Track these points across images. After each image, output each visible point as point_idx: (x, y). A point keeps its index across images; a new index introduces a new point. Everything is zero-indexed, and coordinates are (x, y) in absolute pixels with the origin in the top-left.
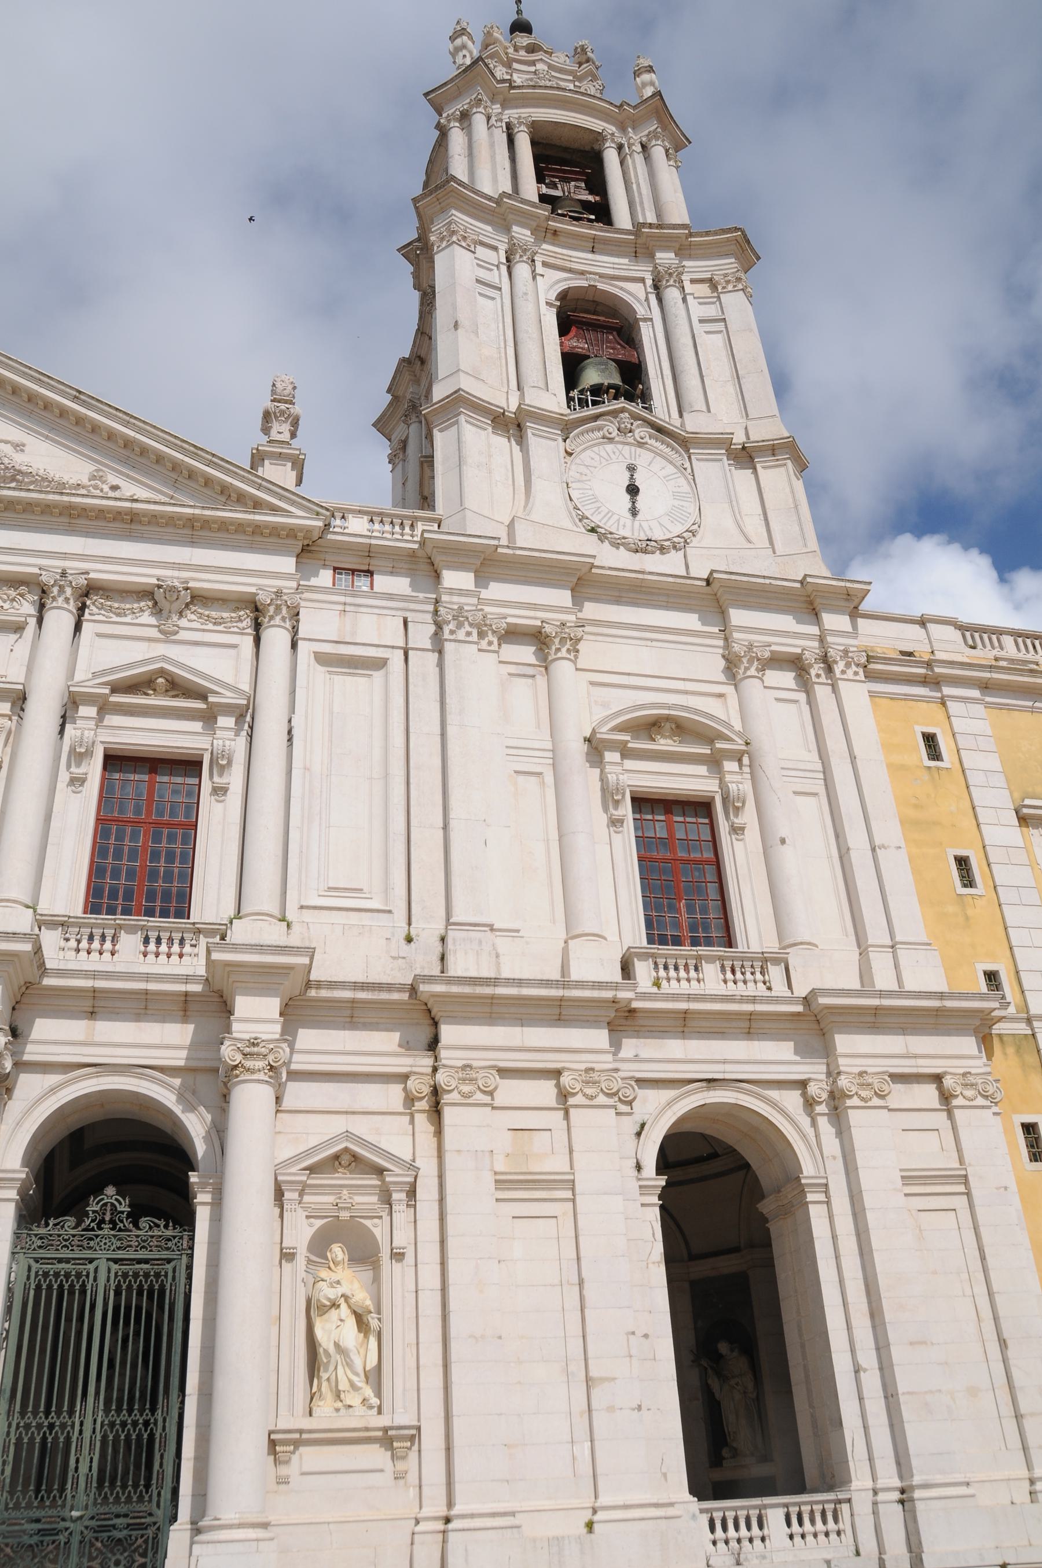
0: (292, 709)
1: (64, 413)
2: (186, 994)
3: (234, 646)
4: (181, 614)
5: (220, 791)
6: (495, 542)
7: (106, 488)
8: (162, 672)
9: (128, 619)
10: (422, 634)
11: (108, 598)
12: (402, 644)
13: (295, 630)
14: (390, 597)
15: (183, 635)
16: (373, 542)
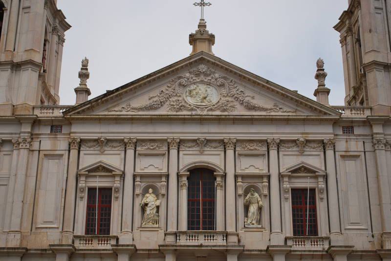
0: (336, 174)
1: (263, 86)
2: (322, 254)
3: (319, 155)
4: (304, 147)
5: (322, 199)
6: (388, 117)
7: (278, 108)
8: (303, 166)
9: (290, 150)
10: (368, 147)
11: (284, 144)
12: (363, 150)
13: (334, 149)
14: (359, 135)
15: (306, 153)
16: (354, 119)
